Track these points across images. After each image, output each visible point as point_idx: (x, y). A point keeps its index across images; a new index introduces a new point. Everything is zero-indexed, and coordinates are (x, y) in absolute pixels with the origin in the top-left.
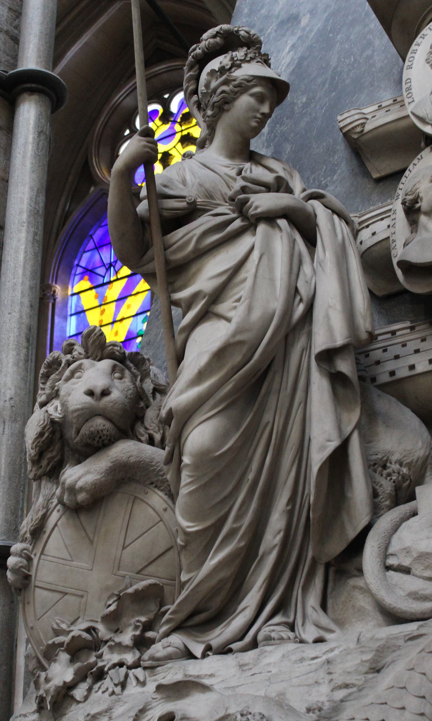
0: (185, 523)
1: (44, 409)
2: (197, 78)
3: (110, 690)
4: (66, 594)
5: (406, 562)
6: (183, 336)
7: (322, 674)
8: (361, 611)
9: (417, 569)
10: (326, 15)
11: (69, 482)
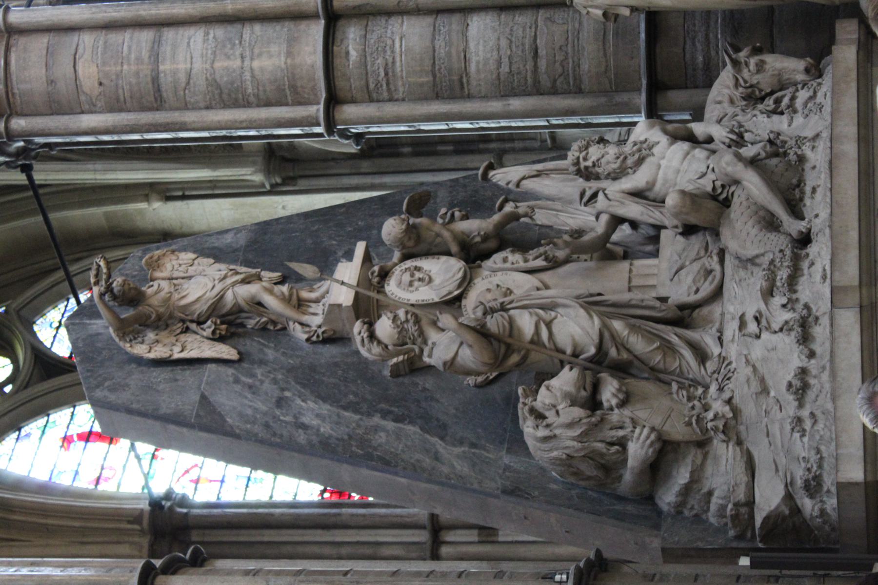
0: (655, 346)
1: (560, 412)
2: (379, 342)
3: (731, 374)
4: (670, 416)
5: (694, 288)
6: (551, 341)
7: (744, 284)
8: (710, 312)
9: (699, 285)
10: (293, 383)
11: (613, 390)
